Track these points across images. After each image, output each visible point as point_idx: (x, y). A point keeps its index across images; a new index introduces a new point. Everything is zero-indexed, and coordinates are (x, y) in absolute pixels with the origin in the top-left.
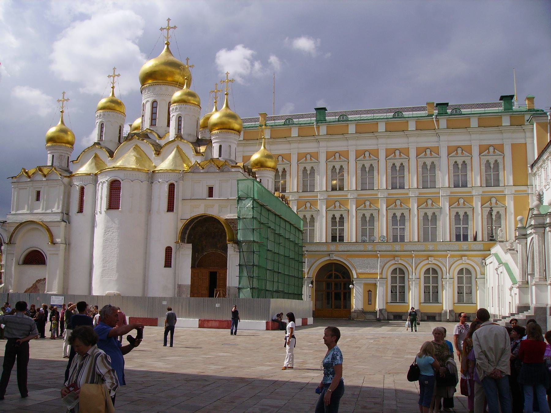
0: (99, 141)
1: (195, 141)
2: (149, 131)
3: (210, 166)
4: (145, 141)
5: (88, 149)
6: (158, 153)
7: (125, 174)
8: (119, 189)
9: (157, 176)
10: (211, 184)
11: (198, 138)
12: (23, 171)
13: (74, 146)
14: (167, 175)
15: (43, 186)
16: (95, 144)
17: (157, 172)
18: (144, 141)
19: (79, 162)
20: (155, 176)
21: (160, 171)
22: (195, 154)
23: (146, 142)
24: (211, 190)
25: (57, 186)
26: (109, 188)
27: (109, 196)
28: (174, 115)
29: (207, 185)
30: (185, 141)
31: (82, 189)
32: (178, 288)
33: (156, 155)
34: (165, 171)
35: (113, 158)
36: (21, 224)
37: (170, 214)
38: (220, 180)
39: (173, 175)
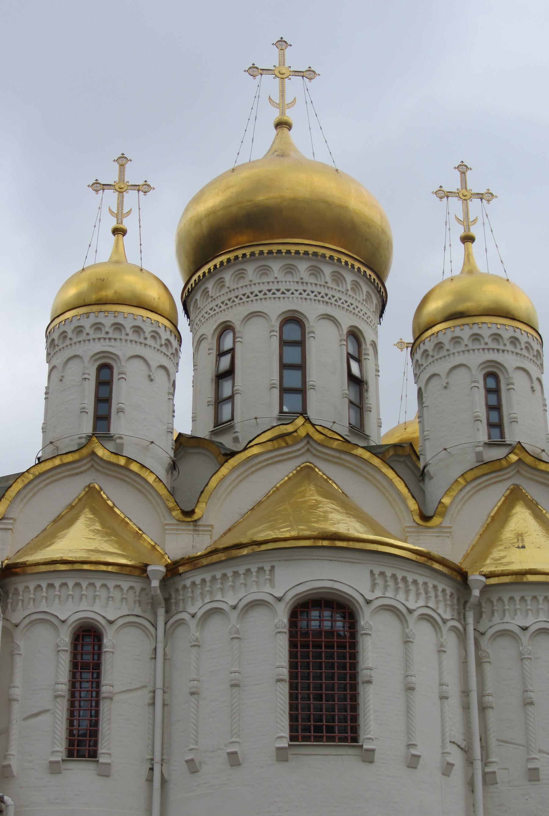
7: (371, 572)
21: (531, 578)
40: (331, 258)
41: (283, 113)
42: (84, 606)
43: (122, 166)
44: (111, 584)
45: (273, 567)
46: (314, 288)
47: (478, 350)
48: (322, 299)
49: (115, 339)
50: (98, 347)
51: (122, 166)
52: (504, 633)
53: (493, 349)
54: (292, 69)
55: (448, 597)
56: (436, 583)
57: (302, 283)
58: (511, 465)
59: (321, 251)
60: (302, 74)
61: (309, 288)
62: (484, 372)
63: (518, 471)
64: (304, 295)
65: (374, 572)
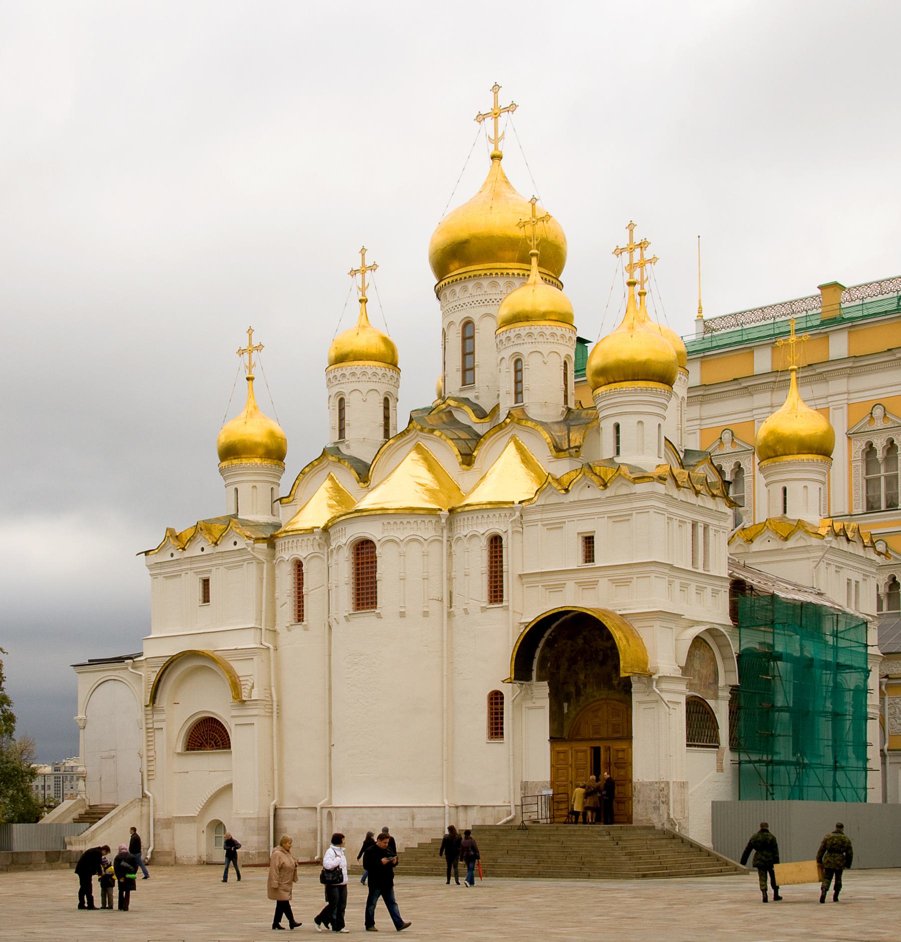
1: (562, 419)
2: (452, 403)
4: (437, 433)
6: (468, 459)
8: (373, 561)
9: (460, 520)
10: (586, 527)
11: (569, 410)
12: (168, 534)
15: (215, 568)
17: (459, 510)
18: (435, 433)
20: (457, 521)
21: (467, 509)
23: (440, 436)
24: (589, 541)
26: (352, 561)
27: (352, 581)
28: (503, 358)
30: (529, 424)
31: (299, 565)
32: (521, 790)
33: (464, 467)
34: (477, 507)
35: (367, 482)
36: (171, 663)
37: (496, 612)
38: (608, 517)
44: (305, 539)
52: (459, 539)
53: (517, 344)
63: (514, 427)
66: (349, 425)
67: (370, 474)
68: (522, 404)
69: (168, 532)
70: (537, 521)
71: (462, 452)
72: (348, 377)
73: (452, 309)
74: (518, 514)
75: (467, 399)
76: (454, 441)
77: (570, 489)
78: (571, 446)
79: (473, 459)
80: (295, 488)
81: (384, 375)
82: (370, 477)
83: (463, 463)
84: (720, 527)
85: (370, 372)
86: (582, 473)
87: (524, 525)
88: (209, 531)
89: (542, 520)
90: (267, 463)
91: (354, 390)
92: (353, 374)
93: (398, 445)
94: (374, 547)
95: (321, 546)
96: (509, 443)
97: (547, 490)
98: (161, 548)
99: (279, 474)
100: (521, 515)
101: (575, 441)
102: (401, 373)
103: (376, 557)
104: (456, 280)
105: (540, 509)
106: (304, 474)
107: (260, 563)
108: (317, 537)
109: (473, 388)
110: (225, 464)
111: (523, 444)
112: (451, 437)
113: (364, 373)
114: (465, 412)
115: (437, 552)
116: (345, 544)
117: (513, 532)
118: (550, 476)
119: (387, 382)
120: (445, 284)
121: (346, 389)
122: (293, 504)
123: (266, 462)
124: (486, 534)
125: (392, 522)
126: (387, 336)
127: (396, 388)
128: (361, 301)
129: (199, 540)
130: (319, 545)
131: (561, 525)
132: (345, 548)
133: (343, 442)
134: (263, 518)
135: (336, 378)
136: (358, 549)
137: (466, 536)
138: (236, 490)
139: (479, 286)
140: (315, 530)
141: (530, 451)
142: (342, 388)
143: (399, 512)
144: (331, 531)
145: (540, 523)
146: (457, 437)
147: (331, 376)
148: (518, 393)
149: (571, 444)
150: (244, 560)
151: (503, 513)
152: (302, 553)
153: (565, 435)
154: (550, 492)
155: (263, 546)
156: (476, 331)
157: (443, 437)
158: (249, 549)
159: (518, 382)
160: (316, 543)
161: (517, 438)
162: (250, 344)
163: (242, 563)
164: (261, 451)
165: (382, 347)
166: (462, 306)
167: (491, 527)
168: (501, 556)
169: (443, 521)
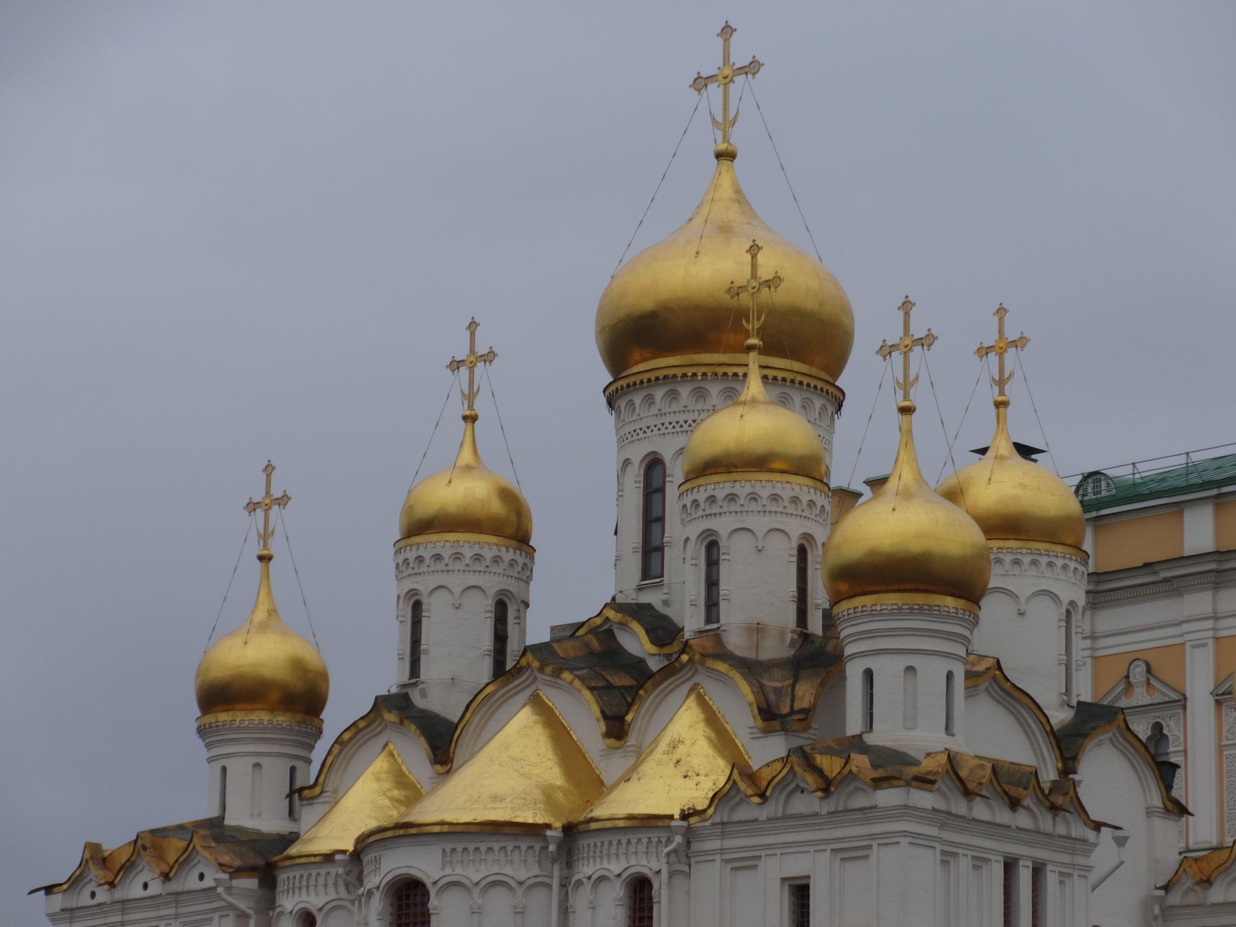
0: (404, 686)
2: (610, 614)
3: (793, 785)
5: (353, 729)
6: (616, 728)
7: (444, 850)
9: (583, 847)
10: (796, 867)
11: (805, 637)
12: (87, 856)
13: (322, 717)
14: (619, 841)
16: (381, 703)
17: (581, 828)
19: (321, 793)
20: (579, 850)
21: (593, 826)
22: (760, 723)
23: (571, 683)
24: (800, 893)
25: (211, 919)
28: (687, 539)
29: (783, 880)
33: (611, 742)
34: (609, 824)
35: (447, 765)
38: (833, 850)
39: (645, 841)
40: (684, 375)
41: (726, 139)
42: (304, 897)
43: (472, 334)
44: (323, 871)
45: (380, 856)
46: (673, 418)
47: (699, 517)
48: (681, 429)
49: (420, 574)
50: (409, 585)
51: (472, 334)
52: (579, 883)
53: (710, 515)
54: (735, 67)
55: (537, 853)
56: (516, 844)
57: (661, 414)
58: (684, 666)
59: (671, 372)
60: (747, 69)
61: (666, 420)
62: (705, 543)
64: (663, 431)
65: (446, 850)
66: (427, 651)
67: (452, 749)
68: (715, 626)
69: (87, 851)
70: (714, 852)
71: (609, 714)
72: (427, 561)
73: (629, 436)
74: (678, 839)
75: (649, 606)
76: (595, 692)
77: (768, 793)
78: (796, 709)
79: (626, 727)
80: (325, 770)
81: (496, 560)
82: (452, 755)
83: (608, 735)
84: (1073, 866)
85: (468, 553)
86: (788, 766)
87: (693, 860)
88: (160, 855)
89: (722, 851)
90: (282, 719)
91: (440, 587)
92: (438, 557)
93: (502, 696)
94: (426, 894)
95: (351, 888)
96: (687, 697)
97: (733, 792)
98: (75, 881)
99: (307, 740)
100: (688, 843)
101: (803, 699)
102: (536, 555)
103: (429, 915)
104: (635, 384)
105: (718, 830)
106: (341, 744)
107: (243, 916)
108: (341, 871)
109: (659, 585)
110: (210, 719)
111: (711, 703)
112: (593, 684)
113: (458, 557)
114: (633, 633)
115: (543, 906)
116: (378, 888)
117: (671, 874)
118: (735, 770)
119: (502, 572)
120: (622, 386)
121: (423, 584)
122: (321, 800)
123: (280, 718)
124: (625, 875)
125: (460, 848)
126: (511, 484)
127: (523, 585)
128: (465, 418)
129: (140, 868)
130: (347, 885)
131: (753, 863)
132: (377, 896)
133: (415, 684)
134: (271, 823)
135: (408, 564)
136: (400, 898)
137: (589, 878)
138: (224, 769)
139: (673, 395)
140: (338, 857)
141: (723, 716)
142: (418, 582)
143: (472, 828)
144: (366, 859)
145: (718, 858)
146: (601, 683)
147: (400, 559)
148: (712, 606)
149: (795, 705)
150: (214, 910)
151: (655, 836)
152: (314, 900)
153: (787, 687)
154: (737, 799)
155: (251, 883)
156: (667, 479)
157: (577, 683)
158: (220, 890)
159: (712, 584)
160: (341, 883)
161: (702, 691)
162: (268, 492)
163: (209, 916)
164: (274, 696)
165: (497, 507)
166: (645, 432)
167: (633, 862)
168: (651, 918)
169: (552, 848)
